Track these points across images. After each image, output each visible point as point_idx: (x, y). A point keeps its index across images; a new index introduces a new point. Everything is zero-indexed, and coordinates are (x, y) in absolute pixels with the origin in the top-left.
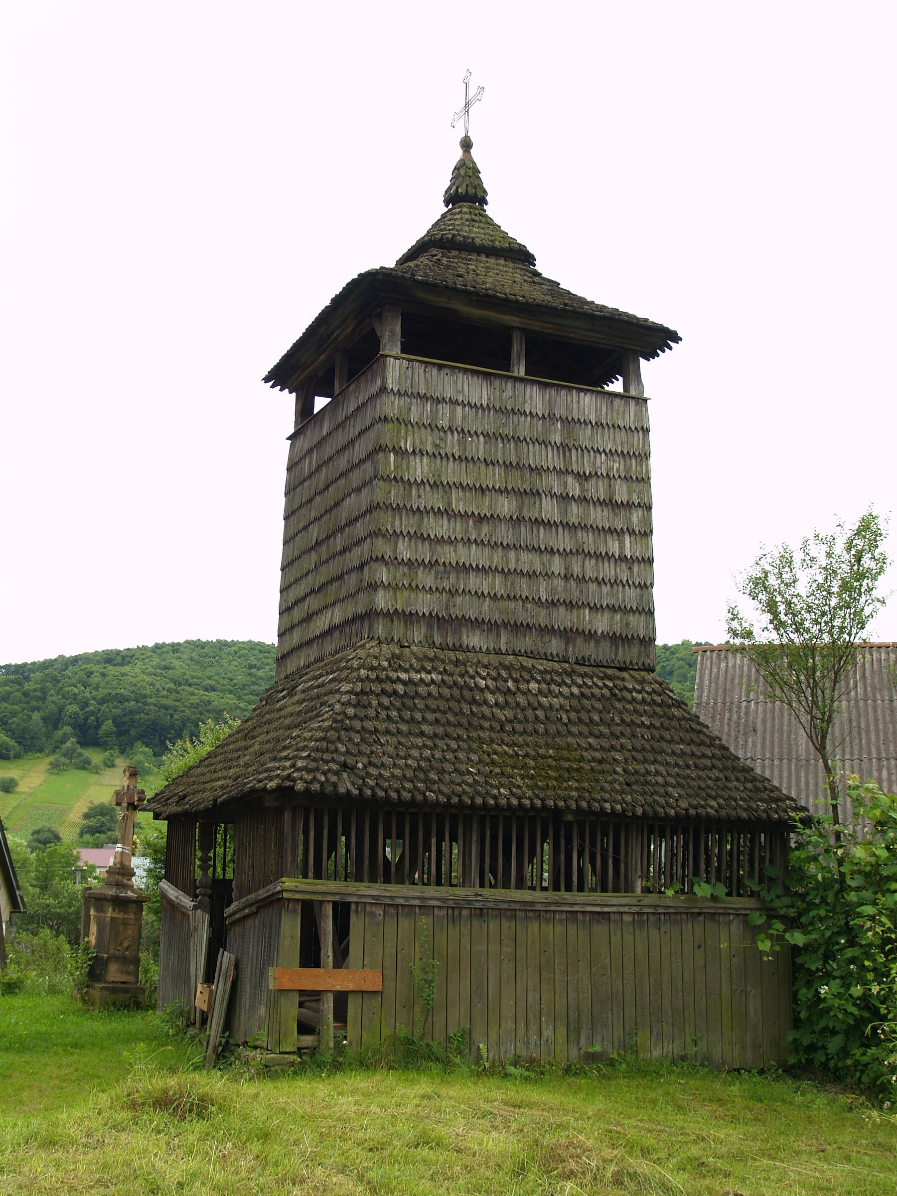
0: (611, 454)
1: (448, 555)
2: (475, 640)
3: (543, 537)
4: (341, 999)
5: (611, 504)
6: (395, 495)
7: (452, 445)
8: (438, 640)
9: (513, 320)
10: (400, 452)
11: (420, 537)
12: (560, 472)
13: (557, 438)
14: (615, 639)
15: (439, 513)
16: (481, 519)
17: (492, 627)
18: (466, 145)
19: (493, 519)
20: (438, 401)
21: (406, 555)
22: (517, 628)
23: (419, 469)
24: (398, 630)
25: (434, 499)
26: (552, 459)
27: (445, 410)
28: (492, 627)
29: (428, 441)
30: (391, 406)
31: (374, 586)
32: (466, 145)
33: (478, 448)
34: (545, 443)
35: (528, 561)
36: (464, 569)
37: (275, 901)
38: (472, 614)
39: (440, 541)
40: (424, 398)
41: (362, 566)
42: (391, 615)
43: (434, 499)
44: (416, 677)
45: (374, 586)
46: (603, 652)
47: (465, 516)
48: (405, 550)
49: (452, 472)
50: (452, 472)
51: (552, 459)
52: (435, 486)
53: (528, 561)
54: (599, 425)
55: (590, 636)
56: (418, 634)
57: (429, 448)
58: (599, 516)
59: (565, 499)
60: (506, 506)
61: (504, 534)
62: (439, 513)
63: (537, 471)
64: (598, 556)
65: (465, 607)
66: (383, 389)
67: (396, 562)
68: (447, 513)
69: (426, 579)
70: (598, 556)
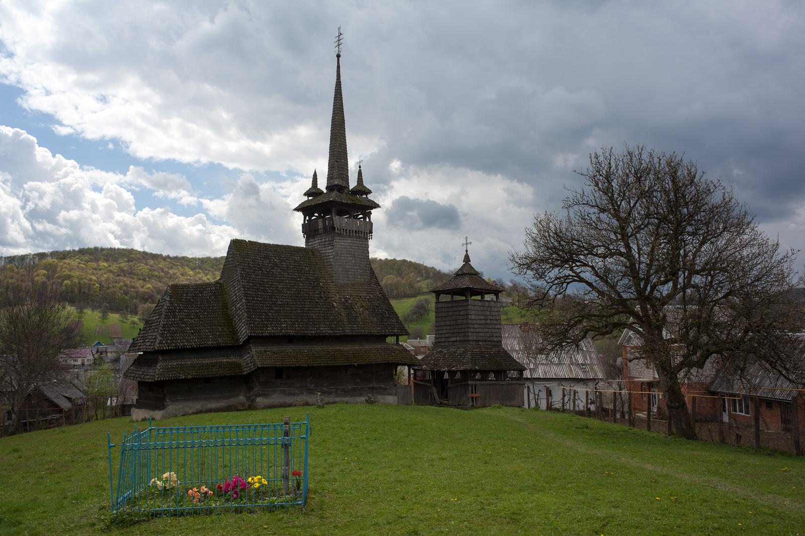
0: (496, 312)
1: (477, 330)
2: (481, 343)
3: (488, 326)
4: (476, 397)
5: (496, 320)
6: (470, 321)
9: (484, 291)
10: (471, 315)
12: (490, 315)
13: (489, 310)
14: (498, 342)
17: (482, 341)
18: (467, 251)
20: (475, 306)
21: (472, 331)
22: (486, 341)
23: (473, 317)
26: (489, 313)
27: (476, 307)
28: (482, 341)
30: (470, 307)
31: (468, 336)
32: (467, 251)
33: (480, 313)
34: (488, 311)
35: (486, 330)
36: (479, 332)
38: (480, 339)
39: (476, 328)
41: (465, 332)
42: (470, 340)
45: (468, 336)
46: (496, 343)
48: (472, 331)
49: (477, 317)
51: (489, 313)
53: (486, 330)
54: (494, 307)
55: (494, 341)
58: (495, 322)
59: (491, 320)
60: (484, 322)
61: (483, 326)
63: (487, 316)
64: (495, 329)
65: (479, 338)
66: (468, 305)
68: (477, 324)
69: (475, 334)
70: (495, 329)
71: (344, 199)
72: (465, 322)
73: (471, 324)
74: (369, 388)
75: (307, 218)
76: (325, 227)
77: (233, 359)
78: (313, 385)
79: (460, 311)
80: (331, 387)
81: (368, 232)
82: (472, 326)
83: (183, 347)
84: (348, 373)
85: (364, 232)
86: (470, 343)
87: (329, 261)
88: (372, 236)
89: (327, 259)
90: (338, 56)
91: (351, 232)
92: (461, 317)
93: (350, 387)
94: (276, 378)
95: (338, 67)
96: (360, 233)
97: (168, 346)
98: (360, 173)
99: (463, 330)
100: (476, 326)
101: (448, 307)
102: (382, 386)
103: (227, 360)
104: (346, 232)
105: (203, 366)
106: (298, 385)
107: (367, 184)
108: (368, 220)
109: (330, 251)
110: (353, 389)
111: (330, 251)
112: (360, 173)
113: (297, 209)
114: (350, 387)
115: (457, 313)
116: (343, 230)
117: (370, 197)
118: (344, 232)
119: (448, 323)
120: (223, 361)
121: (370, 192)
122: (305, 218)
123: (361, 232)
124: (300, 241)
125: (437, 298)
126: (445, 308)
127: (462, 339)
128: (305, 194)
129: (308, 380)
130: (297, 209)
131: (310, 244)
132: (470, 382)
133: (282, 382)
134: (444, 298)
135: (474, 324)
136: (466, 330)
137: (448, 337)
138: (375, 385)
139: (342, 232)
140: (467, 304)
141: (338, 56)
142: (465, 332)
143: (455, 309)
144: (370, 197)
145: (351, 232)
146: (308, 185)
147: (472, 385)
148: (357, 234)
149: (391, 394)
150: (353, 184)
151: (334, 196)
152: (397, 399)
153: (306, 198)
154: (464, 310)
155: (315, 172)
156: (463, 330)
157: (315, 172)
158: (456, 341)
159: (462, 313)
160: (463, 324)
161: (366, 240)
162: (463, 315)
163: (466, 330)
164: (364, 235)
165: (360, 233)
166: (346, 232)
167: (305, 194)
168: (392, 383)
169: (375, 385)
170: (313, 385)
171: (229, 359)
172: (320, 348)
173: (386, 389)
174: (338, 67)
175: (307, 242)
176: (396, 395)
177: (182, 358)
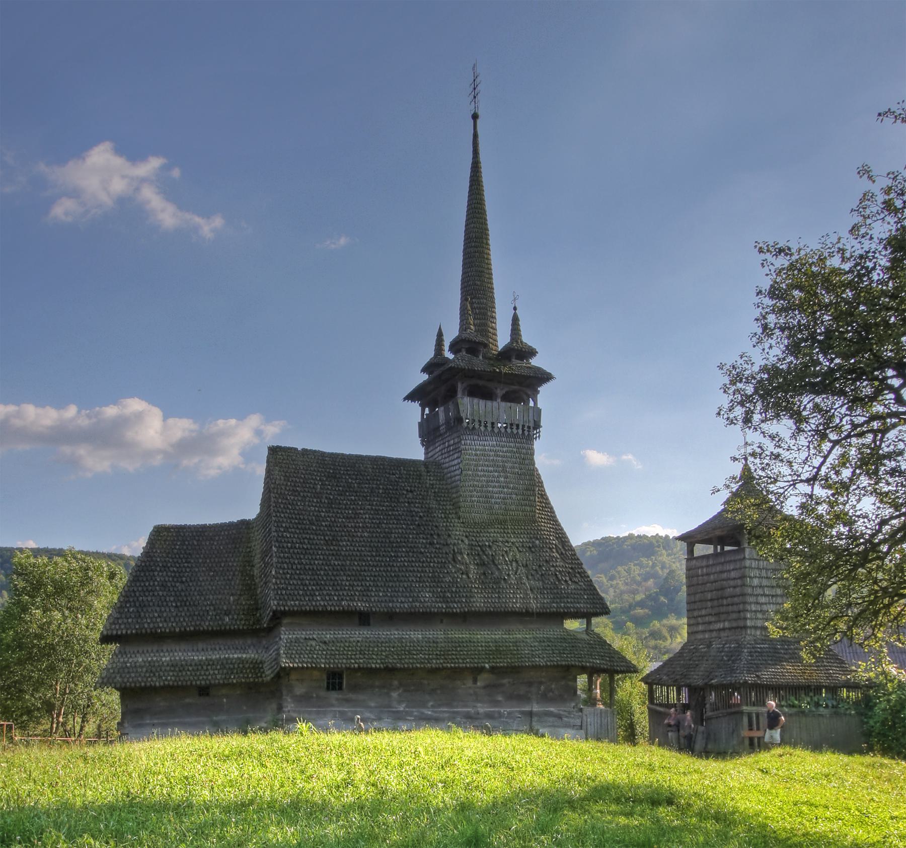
6: (749, 591)
7: (764, 574)
8: (763, 633)
10: (750, 577)
11: (757, 603)
15: (762, 595)
16: (773, 596)
19: (776, 596)
21: (754, 609)
24: (753, 632)
25: (760, 591)
29: (757, 573)
30: (748, 563)
37: (742, 713)
39: (762, 604)
40: (755, 559)
41: (739, 612)
42: (750, 628)
43: (760, 591)
44: (762, 646)
47: (768, 596)
48: (753, 608)
49: (765, 582)
50: (765, 582)
52: (760, 587)
56: (758, 633)
57: (758, 575)
62: (762, 595)
66: (744, 558)
67: (751, 611)
68: (764, 595)
71: (479, 363)
72: (738, 590)
73: (751, 595)
74: (523, 713)
75: (427, 411)
76: (447, 422)
77: (250, 655)
78: (404, 705)
79: (729, 571)
81: (532, 425)
82: (752, 599)
83: (153, 630)
84: (479, 684)
85: (523, 426)
86: (749, 632)
87: (455, 481)
88: (540, 432)
89: (451, 477)
92: (732, 583)
93: (481, 710)
94: (328, 689)
96: (515, 427)
97: (127, 629)
98: (515, 321)
99: (735, 608)
100: (763, 600)
101: (707, 566)
102: (552, 709)
103: (240, 656)
104: (486, 426)
105: (191, 665)
106: (373, 704)
107: (528, 338)
108: (532, 404)
109: (456, 462)
110: (490, 716)
111: (456, 462)
112: (515, 321)
113: (411, 397)
115: (725, 575)
116: (480, 422)
117: (535, 362)
118: (480, 425)
119: (709, 596)
120: (231, 656)
121: (532, 353)
122: (423, 411)
123: (518, 426)
124: (415, 451)
125: (691, 551)
126: (702, 567)
127: (734, 624)
128: (425, 370)
129: (395, 695)
130: (411, 397)
131: (430, 454)
132: (745, 708)
133: (340, 696)
134: (701, 550)
135: (757, 595)
136: (741, 607)
137: (710, 623)
138: (536, 708)
139: (477, 426)
140: (742, 557)
142: (739, 612)
143: (718, 568)
144: (535, 362)
146: (429, 354)
147: (750, 715)
150: (503, 339)
151: (463, 361)
153: (425, 377)
154: (736, 569)
155: (440, 329)
156: (735, 608)
157: (440, 329)
158: (724, 629)
159: (733, 574)
160: (735, 596)
161: (530, 439)
162: (734, 579)
163: (741, 607)
164: (523, 430)
165: (515, 427)
166: (486, 426)
167: (425, 370)
168: (573, 704)
169: (536, 708)
170: (404, 705)
171: (244, 653)
172: (420, 636)
175: (426, 453)
176: (581, 727)
177: (157, 651)
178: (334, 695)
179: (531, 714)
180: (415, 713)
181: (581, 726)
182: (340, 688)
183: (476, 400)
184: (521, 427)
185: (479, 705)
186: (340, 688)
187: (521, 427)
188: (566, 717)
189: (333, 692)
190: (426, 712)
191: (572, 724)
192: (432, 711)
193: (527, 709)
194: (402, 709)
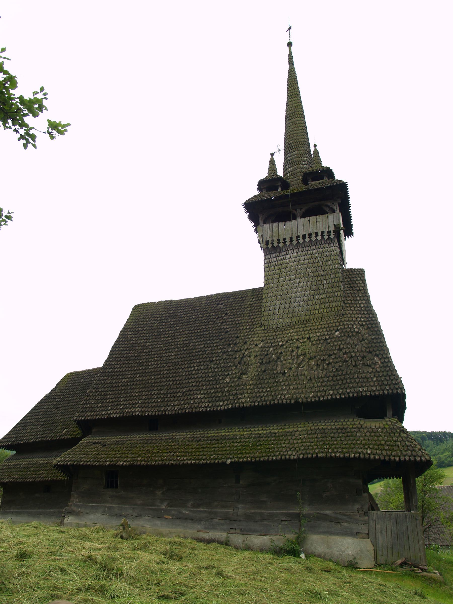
78: (166, 504)
80: (201, 509)
84: (241, 482)
85: (323, 233)
90: (290, 44)
91: (295, 239)
95: (290, 55)
96: (313, 236)
102: (328, 512)
104: (284, 242)
106: (139, 502)
110: (249, 518)
114: (240, 511)
116: (279, 240)
129: (159, 493)
139: (275, 244)
141: (290, 44)
145: (295, 239)
148: (307, 240)
149: (357, 535)
152: (370, 547)
165: (313, 236)
166: (284, 242)
168: (357, 506)
170: (166, 504)
173: (337, 521)
174: (290, 55)
176: (368, 535)
178: (110, 492)
179: (298, 517)
180: (173, 512)
181: (368, 534)
182: (116, 487)
183: (275, 225)
184: (320, 234)
185: (240, 506)
186: (116, 487)
187: (320, 234)
188: (346, 522)
189: (110, 489)
190: (184, 512)
191: (355, 531)
192: (190, 511)
193: (296, 511)
194: (164, 507)
